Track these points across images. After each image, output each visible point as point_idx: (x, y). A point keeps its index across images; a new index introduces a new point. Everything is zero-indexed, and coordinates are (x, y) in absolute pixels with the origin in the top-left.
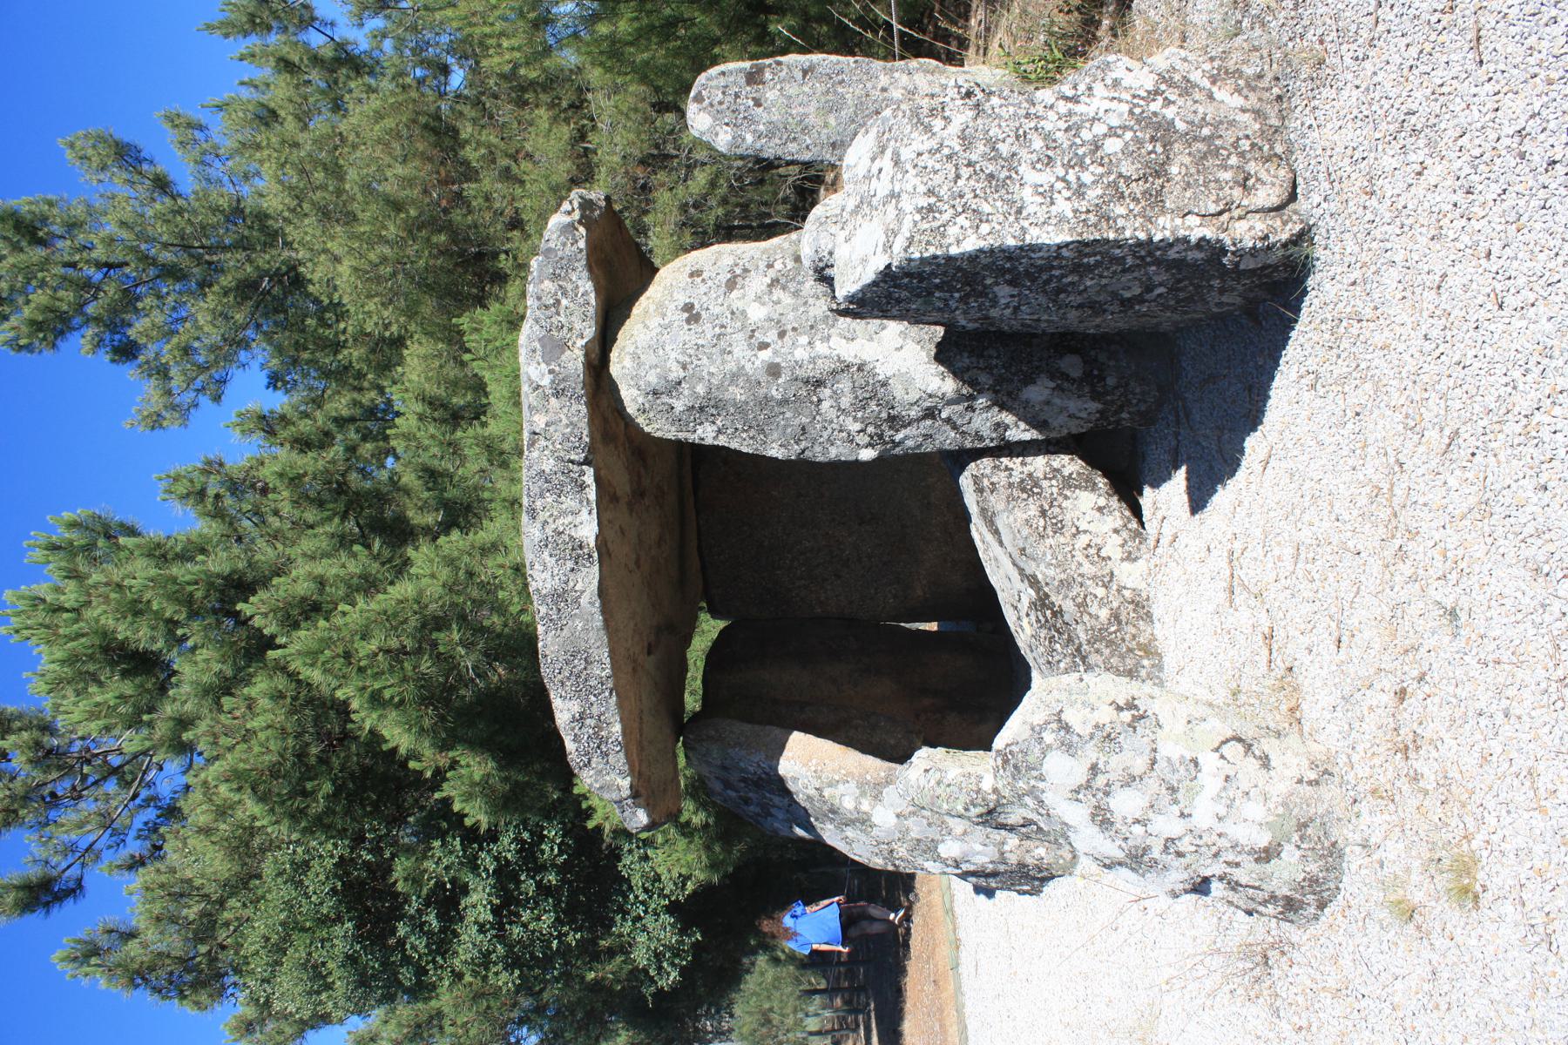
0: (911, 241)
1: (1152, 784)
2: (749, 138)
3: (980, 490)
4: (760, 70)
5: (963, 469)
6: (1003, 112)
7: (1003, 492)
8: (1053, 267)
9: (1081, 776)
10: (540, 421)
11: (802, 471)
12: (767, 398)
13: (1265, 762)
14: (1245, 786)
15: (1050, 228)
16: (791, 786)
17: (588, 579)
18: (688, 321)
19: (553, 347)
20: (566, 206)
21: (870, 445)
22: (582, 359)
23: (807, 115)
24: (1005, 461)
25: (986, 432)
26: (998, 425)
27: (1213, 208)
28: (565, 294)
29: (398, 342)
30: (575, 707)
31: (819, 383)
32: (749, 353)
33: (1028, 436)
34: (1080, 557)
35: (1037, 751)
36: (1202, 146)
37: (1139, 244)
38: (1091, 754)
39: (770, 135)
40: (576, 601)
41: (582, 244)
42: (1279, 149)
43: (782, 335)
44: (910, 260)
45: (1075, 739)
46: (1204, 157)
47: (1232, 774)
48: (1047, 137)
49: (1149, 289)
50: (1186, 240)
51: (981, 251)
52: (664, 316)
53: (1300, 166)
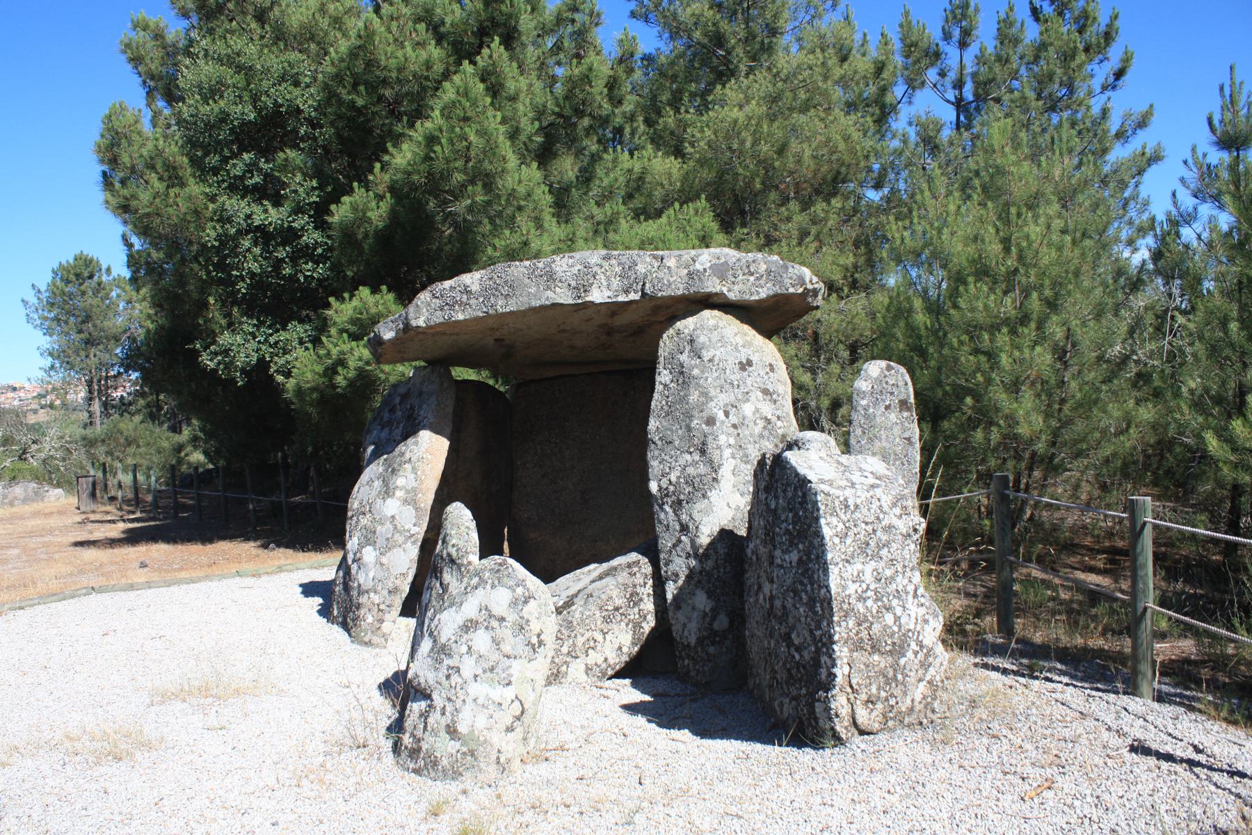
0: (828, 494)
1: (495, 656)
2: (864, 402)
3: (629, 566)
4: (909, 409)
5: (643, 554)
6: (906, 551)
7: (629, 581)
8: (812, 585)
9: (497, 611)
10: (671, 262)
11: (642, 442)
12: (691, 417)
13: (510, 729)
16: (410, 441)
17: (563, 296)
18: (740, 363)
19: (721, 271)
20: (815, 279)
21: (660, 488)
22: (714, 291)
23: (880, 440)
24: (650, 582)
25: (672, 567)
26: (677, 575)
27: (854, 682)
28: (757, 279)
29: (678, 152)
30: (475, 288)
31: (703, 452)
32: (722, 404)
33: (669, 596)
34: (588, 635)
35: (511, 583)
36: (891, 674)
37: (831, 636)
38: (511, 617)
39: (867, 416)
40: (549, 288)
41: (791, 290)
42: (890, 723)
43: (735, 426)
44: (816, 494)
46: (884, 676)
48: (892, 578)
49: (798, 649)
50: (834, 665)
51: (823, 538)
52: (744, 346)
53: (880, 736)
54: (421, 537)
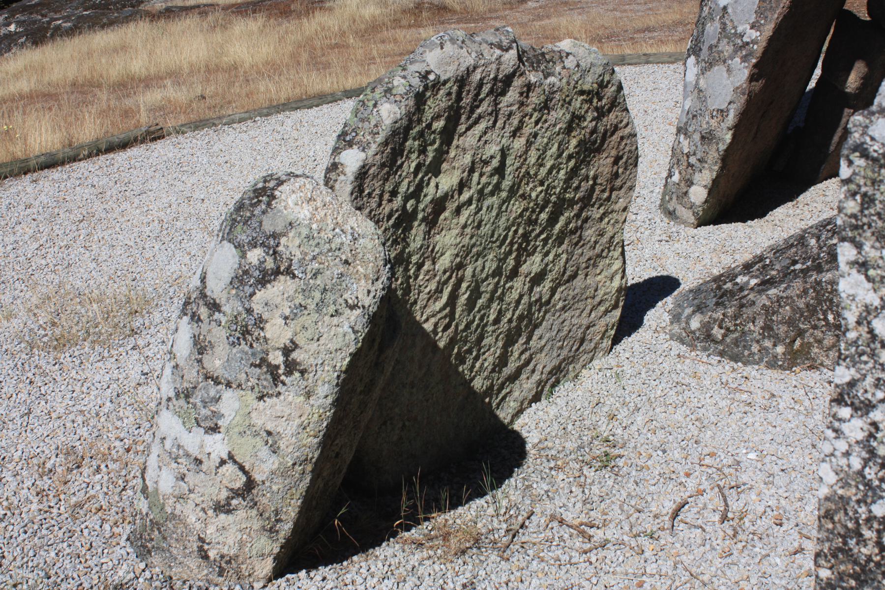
14: (191, 478)
15: (856, 463)
35: (243, 238)
38: (232, 307)
45: (248, 290)
47: (204, 467)
54: (758, 49)
